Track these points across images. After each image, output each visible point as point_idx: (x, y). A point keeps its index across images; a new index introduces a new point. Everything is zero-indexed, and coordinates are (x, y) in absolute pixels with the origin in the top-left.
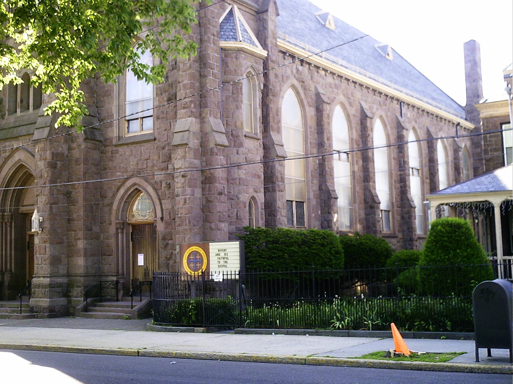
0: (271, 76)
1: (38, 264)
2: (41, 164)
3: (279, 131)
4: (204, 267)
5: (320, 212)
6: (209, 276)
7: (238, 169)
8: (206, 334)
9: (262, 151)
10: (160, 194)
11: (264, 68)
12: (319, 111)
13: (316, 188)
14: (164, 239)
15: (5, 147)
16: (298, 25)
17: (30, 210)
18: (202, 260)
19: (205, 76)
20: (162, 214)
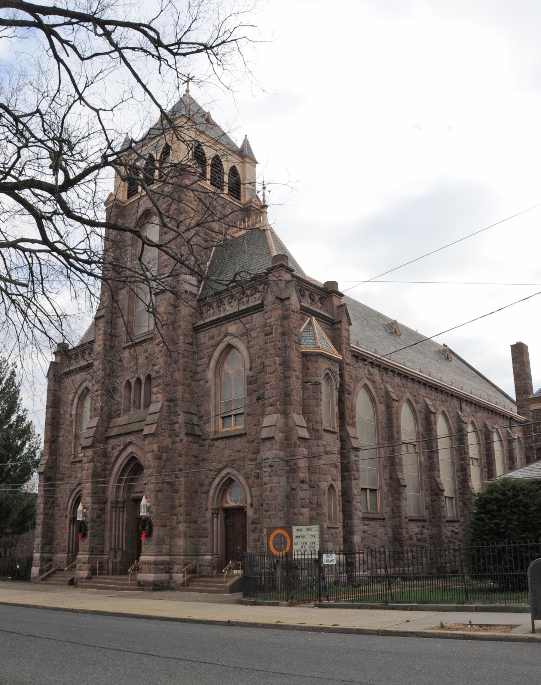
0: (347, 378)
1: (145, 544)
2: (150, 456)
3: (353, 425)
4: (288, 548)
5: (391, 499)
6: (291, 556)
7: (319, 459)
8: (288, 608)
9: (339, 443)
10: (250, 483)
11: (340, 370)
12: (389, 407)
13: (387, 476)
14: (253, 523)
15: (120, 442)
16: (368, 333)
17: (139, 497)
18: (286, 543)
19: (289, 377)
20: (252, 500)
